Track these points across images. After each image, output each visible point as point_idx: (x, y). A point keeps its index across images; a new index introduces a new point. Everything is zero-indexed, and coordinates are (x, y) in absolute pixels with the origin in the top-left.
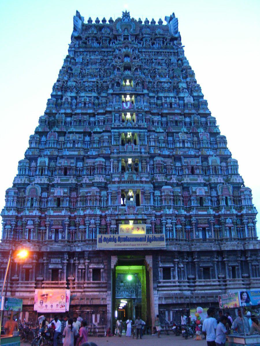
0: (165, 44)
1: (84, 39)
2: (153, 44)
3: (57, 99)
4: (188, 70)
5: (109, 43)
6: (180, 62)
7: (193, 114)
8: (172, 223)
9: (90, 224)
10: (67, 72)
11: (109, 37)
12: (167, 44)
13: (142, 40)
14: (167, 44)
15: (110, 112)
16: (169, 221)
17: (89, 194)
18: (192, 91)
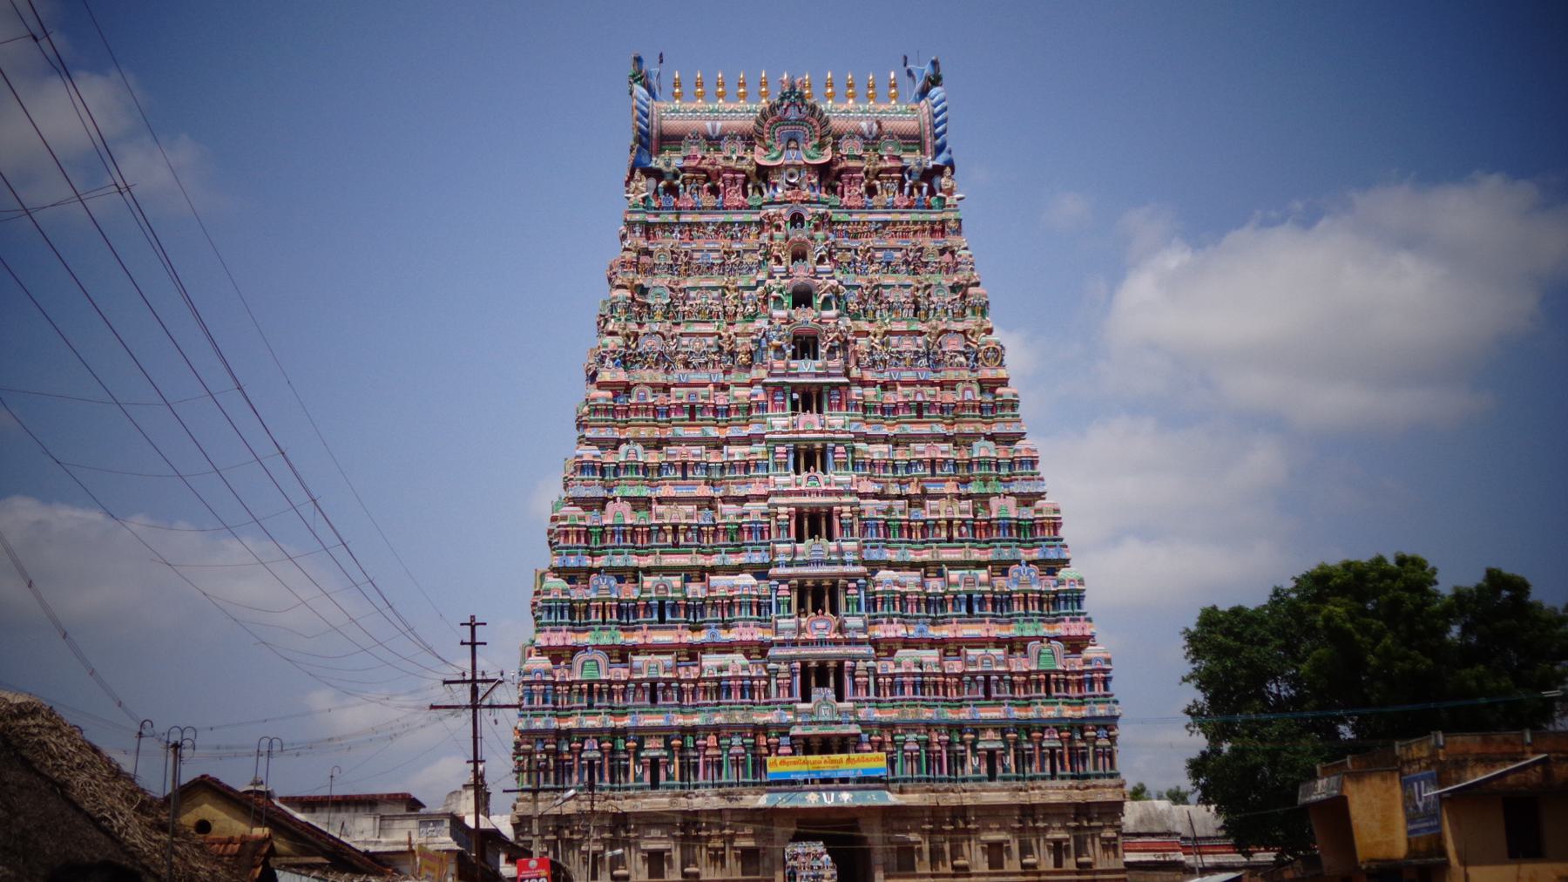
0: (907, 190)
1: (669, 177)
2: (871, 191)
3: (616, 395)
4: (972, 290)
5: (745, 194)
6: (947, 257)
7: (976, 436)
8: (918, 742)
9: (731, 746)
10: (633, 299)
11: (743, 172)
12: (911, 193)
13: (838, 178)
14: (911, 193)
15: (760, 438)
16: (912, 737)
17: (724, 674)
18: (976, 360)
